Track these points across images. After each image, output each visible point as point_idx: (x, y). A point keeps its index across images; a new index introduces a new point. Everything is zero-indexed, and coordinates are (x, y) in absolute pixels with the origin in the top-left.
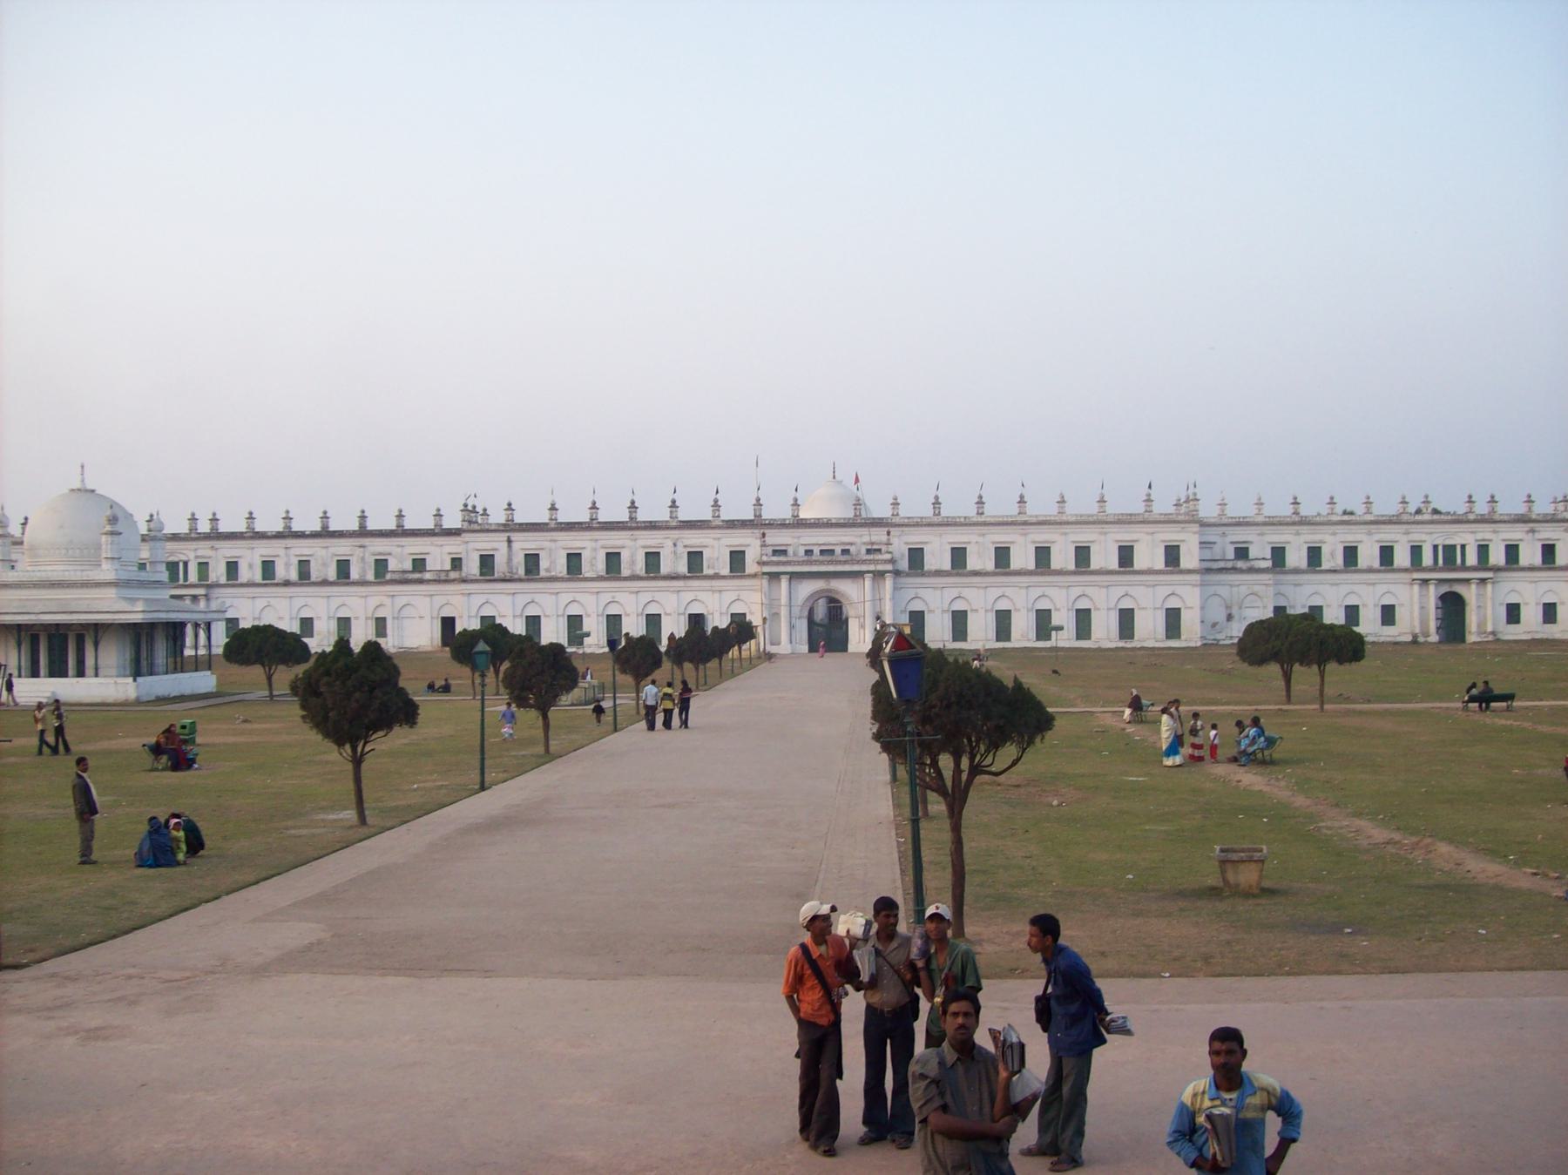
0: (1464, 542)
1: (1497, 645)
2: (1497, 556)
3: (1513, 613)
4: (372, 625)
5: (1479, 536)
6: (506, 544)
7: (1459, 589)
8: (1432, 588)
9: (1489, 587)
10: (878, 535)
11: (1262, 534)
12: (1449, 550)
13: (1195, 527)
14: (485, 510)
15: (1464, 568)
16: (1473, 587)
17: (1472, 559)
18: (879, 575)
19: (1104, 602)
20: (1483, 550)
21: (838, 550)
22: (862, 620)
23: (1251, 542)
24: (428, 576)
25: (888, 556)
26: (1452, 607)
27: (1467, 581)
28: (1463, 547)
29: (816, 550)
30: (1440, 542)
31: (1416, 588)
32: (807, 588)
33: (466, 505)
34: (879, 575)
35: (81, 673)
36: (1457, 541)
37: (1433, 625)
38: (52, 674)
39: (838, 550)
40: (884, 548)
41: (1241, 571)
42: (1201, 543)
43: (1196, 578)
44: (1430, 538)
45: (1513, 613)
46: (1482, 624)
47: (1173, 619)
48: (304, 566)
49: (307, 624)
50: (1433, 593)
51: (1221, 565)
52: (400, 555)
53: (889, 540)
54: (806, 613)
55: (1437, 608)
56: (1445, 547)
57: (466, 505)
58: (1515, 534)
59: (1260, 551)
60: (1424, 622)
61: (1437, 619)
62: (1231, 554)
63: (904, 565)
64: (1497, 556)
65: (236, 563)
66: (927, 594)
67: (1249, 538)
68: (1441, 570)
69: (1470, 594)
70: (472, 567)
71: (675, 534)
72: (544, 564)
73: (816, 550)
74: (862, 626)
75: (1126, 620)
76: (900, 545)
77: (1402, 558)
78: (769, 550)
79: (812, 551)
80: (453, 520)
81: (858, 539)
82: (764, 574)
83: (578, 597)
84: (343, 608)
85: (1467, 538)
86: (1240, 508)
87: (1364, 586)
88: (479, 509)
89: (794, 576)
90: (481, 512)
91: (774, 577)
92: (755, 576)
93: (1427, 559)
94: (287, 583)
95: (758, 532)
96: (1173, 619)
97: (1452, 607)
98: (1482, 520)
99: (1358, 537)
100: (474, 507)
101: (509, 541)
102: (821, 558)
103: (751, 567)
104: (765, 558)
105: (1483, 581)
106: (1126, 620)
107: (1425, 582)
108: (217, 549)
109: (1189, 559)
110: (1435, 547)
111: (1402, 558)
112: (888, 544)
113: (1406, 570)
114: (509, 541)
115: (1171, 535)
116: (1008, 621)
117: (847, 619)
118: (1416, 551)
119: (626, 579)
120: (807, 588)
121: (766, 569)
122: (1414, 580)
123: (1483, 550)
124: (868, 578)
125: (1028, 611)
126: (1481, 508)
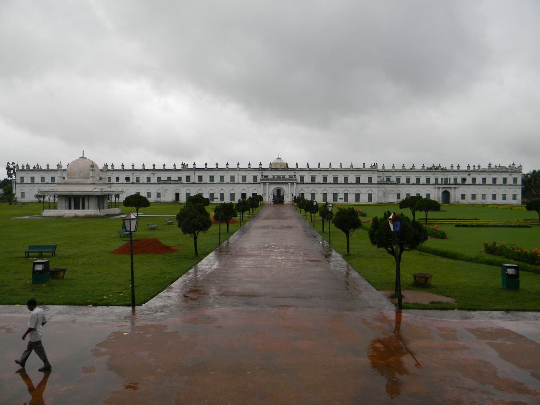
0: (449, 177)
1: (458, 205)
2: (459, 181)
3: (463, 197)
5: (454, 176)
6: (194, 174)
7: (448, 190)
8: (441, 189)
9: (457, 189)
10: (292, 174)
11: (394, 174)
13: (377, 172)
14: (187, 164)
15: (450, 184)
16: (452, 189)
17: (452, 182)
18: (292, 184)
19: (352, 191)
20: (455, 179)
21: (281, 177)
22: (287, 195)
23: (391, 176)
24: (172, 182)
25: (295, 179)
26: (446, 195)
27: (451, 188)
28: (450, 178)
29: (276, 177)
30: (443, 177)
31: (436, 189)
32: (273, 187)
33: (183, 163)
34: (292, 184)
35: (83, 208)
37: (441, 199)
38: (75, 208)
39: (281, 177)
40: (294, 177)
41: (388, 184)
42: (378, 176)
43: (376, 186)
44: (441, 176)
45: (463, 197)
47: (370, 197)
49: (149, 194)
50: (441, 191)
51: (383, 182)
52: (164, 177)
53: (295, 174)
54: (272, 194)
55: (442, 195)
56: (444, 178)
57: (183, 163)
58: (465, 175)
59: (394, 179)
60: (439, 199)
61: (442, 198)
62: (385, 179)
63: (299, 181)
66: (305, 189)
67: (390, 175)
68: (443, 184)
70: (184, 180)
71: (238, 172)
73: (276, 177)
74: (288, 197)
75: (358, 196)
76: (298, 175)
77: (432, 181)
78: (263, 177)
79: (275, 177)
80: (179, 167)
81: (287, 175)
82: (262, 183)
83: (213, 188)
85: (451, 176)
86: (388, 167)
87: (421, 189)
88: (186, 164)
89: (270, 183)
90: (186, 165)
91: (265, 184)
92: (259, 183)
93: (440, 182)
94: (133, 183)
95: (261, 172)
96: (370, 197)
97: (446, 195)
98: (455, 171)
99: (420, 176)
100: (185, 164)
101: (194, 173)
102: (277, 179)
103: (258, 181)
104: (262, 179)
105: (455, 188)
106: (358, 196)
107: (439, 188)
108: (113, 174)
109: (375, 181)
110: (442, 178)
111: (432, 181)
112: (295, 175)
113: (433, 184)
114: (194, 173)
115: (370, 174)
116: (326, 196)
117: (283, 196)
118: (437, 179)
120: (273, 187)
122: (435, 187)
123: (455, 179)
124: (290, 184)
125: (331, 193)
126: (455, 168)
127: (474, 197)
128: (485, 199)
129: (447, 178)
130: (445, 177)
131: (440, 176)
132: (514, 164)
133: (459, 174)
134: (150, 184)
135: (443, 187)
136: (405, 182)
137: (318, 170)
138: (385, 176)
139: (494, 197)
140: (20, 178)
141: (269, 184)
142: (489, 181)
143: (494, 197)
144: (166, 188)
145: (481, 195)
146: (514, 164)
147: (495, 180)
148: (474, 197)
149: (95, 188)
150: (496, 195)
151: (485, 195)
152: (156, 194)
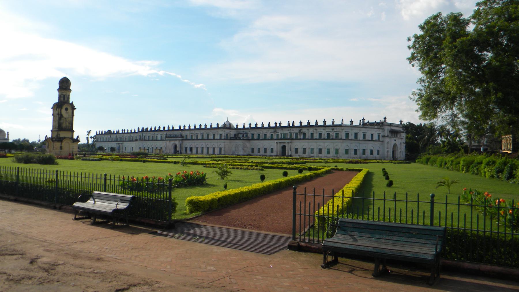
4: (250, 150)
5: (290, 131)
8: (279, 144)
12: (284, 134)
23: (248, 133)
28: (287, 134)
32: (172, 142)
46: (288, 152)
48: (320, 134)
56: (283, 134)
69: (286, 145)
72: (146, 138)
84: (296, 146)
89: (170, 140)
92: (165, 140)
93: (280, 137)
101: (142, 134)
107: (277, 142)
110: (282, 134)
114: (142, 134)
119: (350, 140)
127: (304, 151)
128: (313, 153)
129: (285, 134)
130: (284, 133)
131: (280, 132)
132: (363, 119)
133: (293, 130)
135: (280, 142)
136: (318, 137)
137: (351, 127)
138: (245, 133)
139: (320, 151)
141: (170, 141)
142: (316, 136)
143: (320, 151)
144: (202, 143)
145: (310, 149)
146: (363, 119)
147: (320, 134)
148: (304, 151)
151: (313, 149)
152: (318, 150)
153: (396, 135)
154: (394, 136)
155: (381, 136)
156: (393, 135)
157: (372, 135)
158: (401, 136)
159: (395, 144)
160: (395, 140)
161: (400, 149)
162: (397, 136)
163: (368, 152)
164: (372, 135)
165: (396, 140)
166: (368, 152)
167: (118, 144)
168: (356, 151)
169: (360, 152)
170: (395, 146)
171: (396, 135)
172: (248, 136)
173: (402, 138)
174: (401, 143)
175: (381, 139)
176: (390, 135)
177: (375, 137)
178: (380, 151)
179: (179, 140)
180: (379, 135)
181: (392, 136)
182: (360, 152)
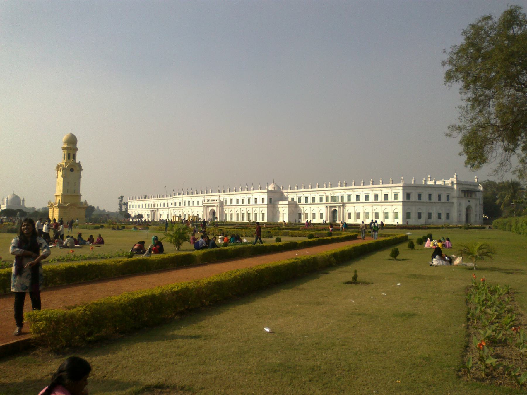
2: (345, 200)
12: (335, 197)
26: (334, 213)
28: (338, 196)
32: (210, 209)
36: (336, 195)
43: (266, 206)
64: (345, 200)
65: (410, 194)
69: (337, 209)
97: (334, 213)
105: (339, 206)
107: (327, 207)
118: (327, 198)
120: (210, 209)
121: (204, 205)
130: (334, 195)
134: (410, 202)
135: (331, 207)
140: (365, 196)
149: (420, 209)
150: (422, 214)
153: (469, 195)
154: (468, 196)
155: (450, 197)
156: (466, 195)
157: (440, 196)
158: (476, 196)
159: (470, 205)
160: (469, 201)
161: (476, 212)
162: (471, 196)
163: (434, 216)
164: (440, 196)
165: (471, 201)
166: (434, 216)
167: (153, 211)
168: (419, 216)
169: (424, 216)
170: (468, 209)
171: (469, 195)
172: (295, 200)
173: (478, 199)
174: (476, 205)
175: (450, 201)
176: (463, 195)
177: (444, 199)
178: (450, 214)
179: (217, 206)
180: (448, 196)
181: (465, 196)
182: (424, 216)
